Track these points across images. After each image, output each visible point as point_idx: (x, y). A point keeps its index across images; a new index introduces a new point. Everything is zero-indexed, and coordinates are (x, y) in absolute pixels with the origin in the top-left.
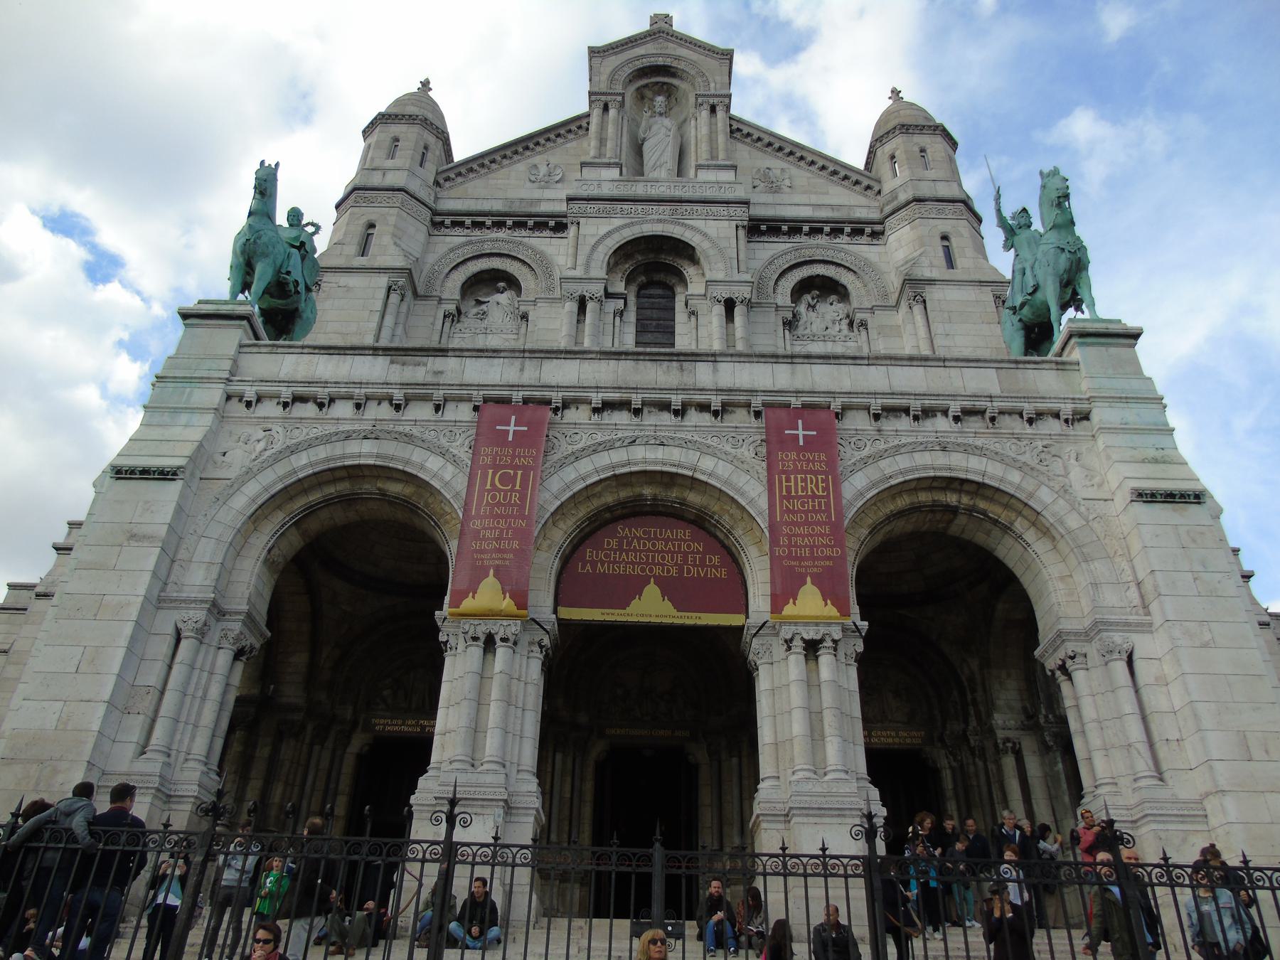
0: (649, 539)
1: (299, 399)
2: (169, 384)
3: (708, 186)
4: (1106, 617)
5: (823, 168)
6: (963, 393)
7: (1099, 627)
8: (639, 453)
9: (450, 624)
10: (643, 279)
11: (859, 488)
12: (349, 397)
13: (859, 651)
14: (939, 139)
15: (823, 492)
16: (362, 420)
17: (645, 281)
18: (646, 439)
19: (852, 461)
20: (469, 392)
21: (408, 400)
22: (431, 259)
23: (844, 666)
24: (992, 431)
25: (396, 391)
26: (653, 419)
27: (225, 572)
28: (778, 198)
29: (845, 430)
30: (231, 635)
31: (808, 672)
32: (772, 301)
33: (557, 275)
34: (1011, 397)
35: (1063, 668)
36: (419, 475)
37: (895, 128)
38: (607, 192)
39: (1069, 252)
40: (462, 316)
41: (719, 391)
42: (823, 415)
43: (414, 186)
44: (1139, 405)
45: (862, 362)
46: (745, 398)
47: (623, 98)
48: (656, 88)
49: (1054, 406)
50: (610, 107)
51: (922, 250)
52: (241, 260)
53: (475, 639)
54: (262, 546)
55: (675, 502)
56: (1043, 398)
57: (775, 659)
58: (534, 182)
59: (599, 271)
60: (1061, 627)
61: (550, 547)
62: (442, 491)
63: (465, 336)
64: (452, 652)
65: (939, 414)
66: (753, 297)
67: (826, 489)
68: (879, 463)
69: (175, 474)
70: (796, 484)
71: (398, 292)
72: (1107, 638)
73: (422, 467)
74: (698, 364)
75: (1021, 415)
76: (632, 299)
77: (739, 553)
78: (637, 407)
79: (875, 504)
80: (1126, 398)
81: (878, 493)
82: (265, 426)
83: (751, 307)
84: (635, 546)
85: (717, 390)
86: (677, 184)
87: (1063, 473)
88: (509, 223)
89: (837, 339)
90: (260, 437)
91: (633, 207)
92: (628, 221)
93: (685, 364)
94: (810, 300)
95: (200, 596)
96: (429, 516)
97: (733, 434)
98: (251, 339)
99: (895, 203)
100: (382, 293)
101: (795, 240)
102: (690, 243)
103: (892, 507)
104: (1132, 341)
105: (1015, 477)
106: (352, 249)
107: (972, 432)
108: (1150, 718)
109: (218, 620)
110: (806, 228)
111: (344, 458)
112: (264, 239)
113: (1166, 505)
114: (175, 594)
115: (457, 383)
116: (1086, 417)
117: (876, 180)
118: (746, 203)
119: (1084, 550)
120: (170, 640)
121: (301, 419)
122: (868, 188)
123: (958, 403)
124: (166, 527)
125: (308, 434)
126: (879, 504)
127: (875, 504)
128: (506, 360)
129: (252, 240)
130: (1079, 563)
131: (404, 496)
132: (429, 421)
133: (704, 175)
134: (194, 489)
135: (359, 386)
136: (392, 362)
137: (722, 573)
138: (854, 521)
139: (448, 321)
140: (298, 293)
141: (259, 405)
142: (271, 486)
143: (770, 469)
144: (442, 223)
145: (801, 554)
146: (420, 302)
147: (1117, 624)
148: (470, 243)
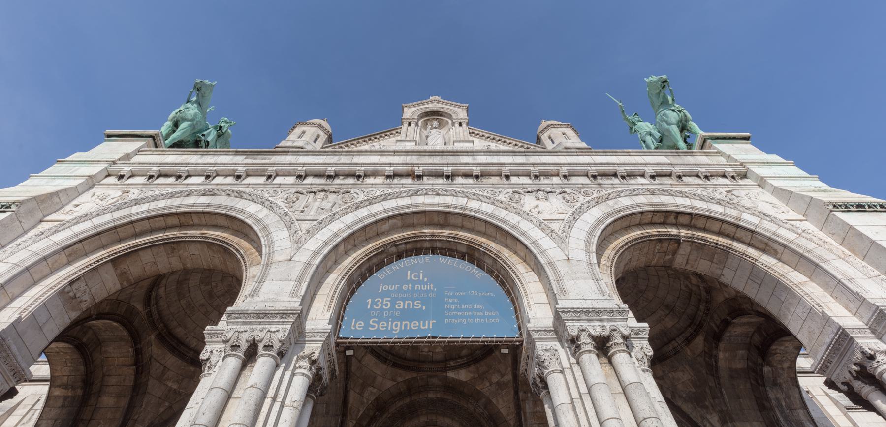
18: (425, 192)
78: (419, 174)
97: (491, 189)
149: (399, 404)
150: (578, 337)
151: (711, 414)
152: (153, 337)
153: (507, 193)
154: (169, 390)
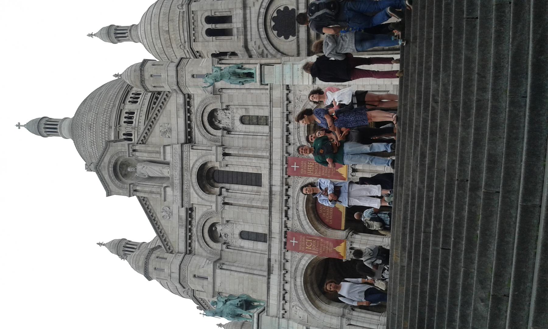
3: (174, 157)
8: (300, 208)
10: (212, 181)
22: (205, 254)
38: (178, 193)
40: (226, 242)
59: (213, 198)
63: (234, 241)
76: (221, 185)
86: (174, 168)
89: (233, 115)
91: (185, 185)
92: (191, 187)
99: (177, 90)
110: (189, 122)
118: (182, 145)
139: (229, 247)
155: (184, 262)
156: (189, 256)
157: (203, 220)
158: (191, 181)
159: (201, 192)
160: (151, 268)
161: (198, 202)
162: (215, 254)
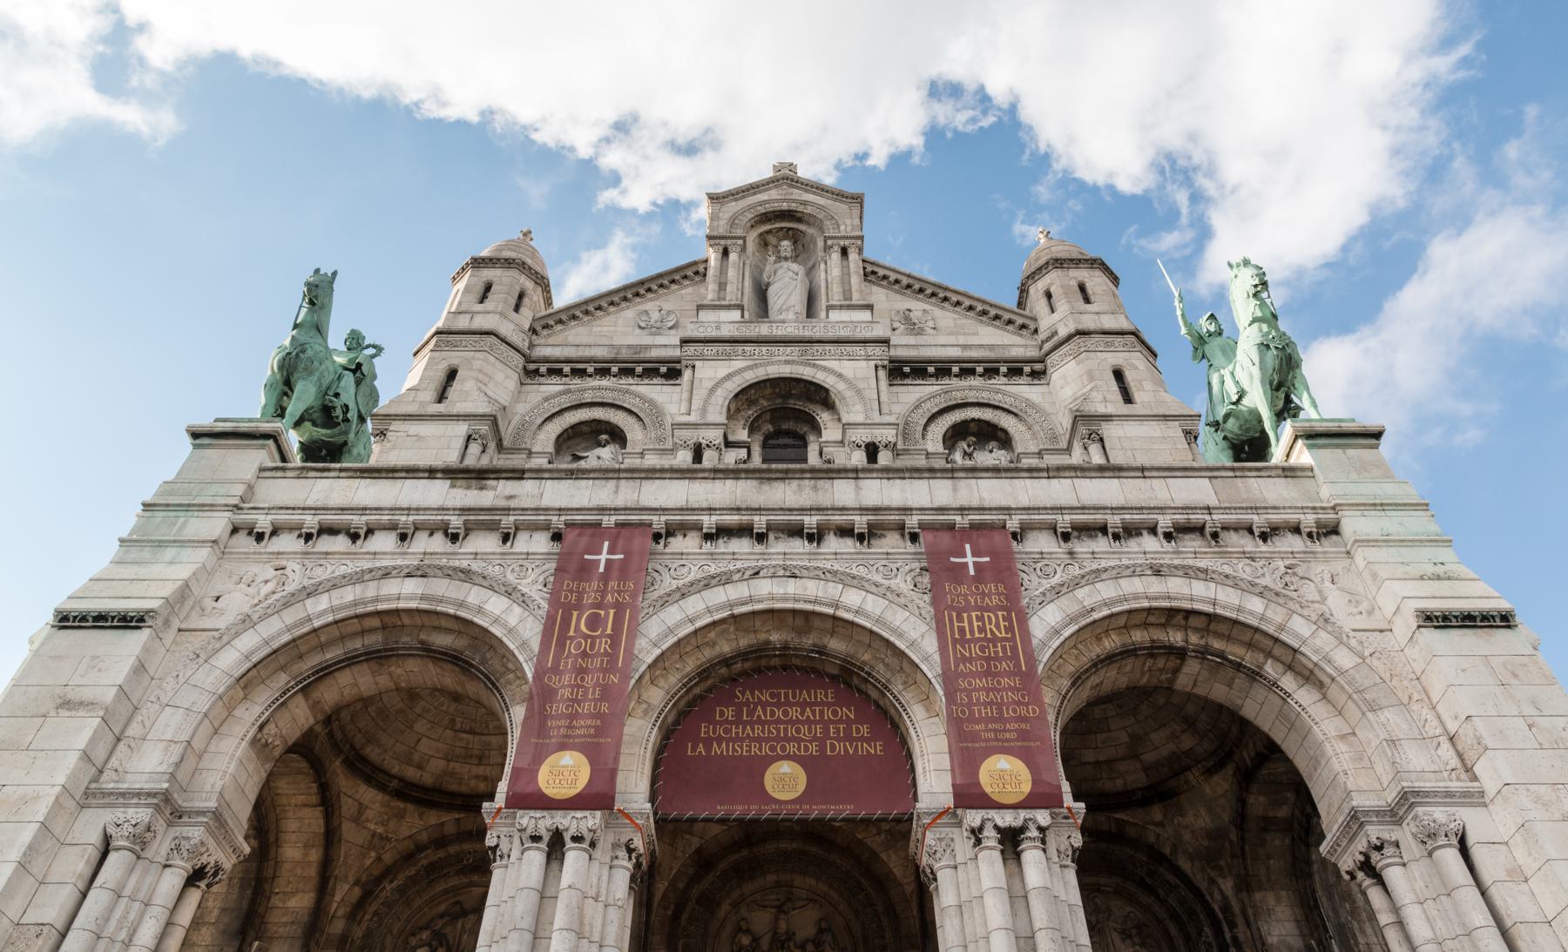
0: (778, 705)
1: (328, 530)
2: (157, 514)
3: (842, 325)
4: (1417, 784)
5: (971, 308)
6: (1173, 505)
7: (1408, 800)
9: (503, 821)
10: (769, 428)
11: (1053, 624)
12: (392, 527)
13: (1076, 845)
14: (1098, 273)
15: (1006, 633)
16: (406, 553)
17: (771, 429)
18: (772, 570)
19: (1041, 590)
20: (548, 518)
21: (469, 529)
22: (521, 408)
23: (1056, 868)
24: (1216, 549)
25: (452, 518)
26: (779, 547)
27: (191, 755)
28: (921, 340)
29: (1027, 553)
30: (185, 845)
31: (1009, 876)
32: (921, 447)
33: (668, 421)
34: (1235, 508)
35: (1367, 866)
36: (476, 620)
37: (1047, 263)
39: (1276, 348)
41: (863, 510)
42: (997, 538)
43: (506, 329)
44: (1399, 513)
45: (1041, 475)
46: (897, 518)
47: (745, 241)
48: (780, 234)
49: (1292, 517)
50: (730, 250)
51: (1092, 384)
52: (278, 376)
53: (536, 838)
54: (252, 719)
55: (813, 651)
56: (1275, 508)
57: (960, 859)
58: (644, 328)
59: (717, 414)
60: (1354, 803)
61: (646, 712)
62: (505, 639)
64: (504, 862)
65: (1145, 533)
66: (899, 443)
67: (1010, 629)
68: (1075, 592)
69: (141, 620)
70: (970, 622)
71: (479, 441)
72: (1425, 814)
73: (480, 610)
74: (836, 481)
75: (1250, 531)
77: (901, 716)
78: (760, 531)
79: (1075, 647)
80: (1382, 505)
81: (1079, 631)
82: (277, 563)
83: (898, 455)
84: (759, 716)
85: (861, 509)
87: (1317, 598)
88: (615, 369)
90: (268, 577)
92: (751, 363)
93: (821, 483)
94: (966, 447)
95: (148, 786)
96: (485, 675)
97: (884, 562)
98: (275, 462)
99: (1056, 338)
100: (460, 443)
101: (943, 382)
102: (823, 384)
103: (1098, 650)
104: (1373, 441)
105: (1255, 605)
106: (429, 395)
107: (1191, 552)
108: (1514, 932)
109: (170, 824)
110: (955, 369)
111: (377, 601)
112: (309, 353)
113: (1466, 631)
114: (111, 785)
115: (532, 506)
116: (1333, 530)
117: (1031, 318)
118: (885, 342)
119: (1367, 696)
120: (93, 853)
121: (327, 553)
122: (1023, 327)
123: (1168, 517)
124: (115, 690)
125: (333, 573)
126: (1080, 646)
127: (1075, 647)
128: (597, 482)
129: (294, 353)
130: (1364, 714)
131: (455, 650)
132: (494, 554)
133: (835, 316)
134: (168, 642)
135: (406, 512)
136: (453, 486)
137: (876, 749)
138: (1049, 668)
140: (346, 420)
141: (274, 539)
142: (273, 638)
143: (935, 602)
144: (536, 372)
145: (987, 713)
146: (504, 456)
147: (1435, 794)
148: (568, 391)
149: (733, 858)
150: (981, 829)
151: (1225, 877)
152: (338, 763)
153: (911, 571)
154: (373, 836)
155: (502, 347)
156: (521, 366)
157: (634, 405)
158: (769, 364)
159: (734, 386)
160: (488, 274)
161: (701, 379)
162: (518, 434)
